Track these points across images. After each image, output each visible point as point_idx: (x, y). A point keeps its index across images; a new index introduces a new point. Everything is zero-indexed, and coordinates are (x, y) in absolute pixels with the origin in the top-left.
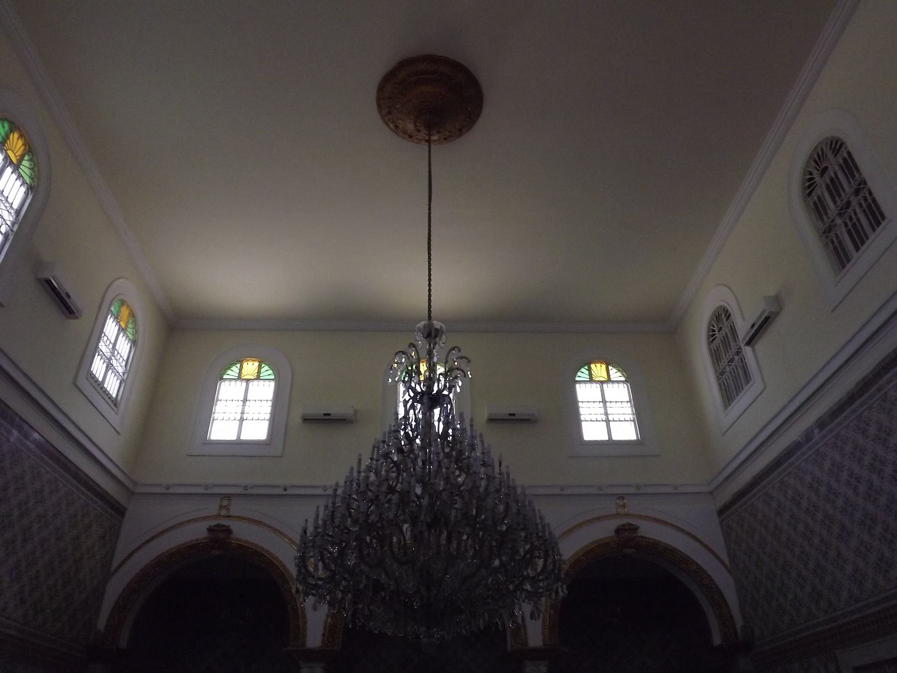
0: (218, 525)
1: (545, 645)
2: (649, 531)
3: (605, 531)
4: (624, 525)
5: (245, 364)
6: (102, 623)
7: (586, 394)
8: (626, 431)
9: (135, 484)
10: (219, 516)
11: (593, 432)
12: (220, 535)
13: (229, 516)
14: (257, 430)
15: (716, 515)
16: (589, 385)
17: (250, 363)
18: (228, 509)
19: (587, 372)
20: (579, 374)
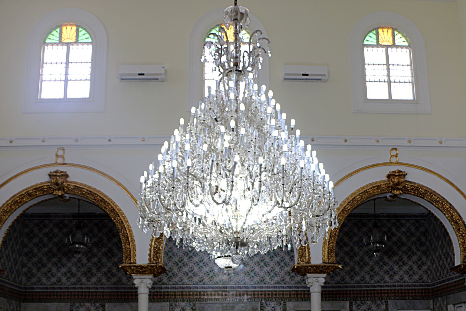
1: (324, 262)
2: (414, 177)
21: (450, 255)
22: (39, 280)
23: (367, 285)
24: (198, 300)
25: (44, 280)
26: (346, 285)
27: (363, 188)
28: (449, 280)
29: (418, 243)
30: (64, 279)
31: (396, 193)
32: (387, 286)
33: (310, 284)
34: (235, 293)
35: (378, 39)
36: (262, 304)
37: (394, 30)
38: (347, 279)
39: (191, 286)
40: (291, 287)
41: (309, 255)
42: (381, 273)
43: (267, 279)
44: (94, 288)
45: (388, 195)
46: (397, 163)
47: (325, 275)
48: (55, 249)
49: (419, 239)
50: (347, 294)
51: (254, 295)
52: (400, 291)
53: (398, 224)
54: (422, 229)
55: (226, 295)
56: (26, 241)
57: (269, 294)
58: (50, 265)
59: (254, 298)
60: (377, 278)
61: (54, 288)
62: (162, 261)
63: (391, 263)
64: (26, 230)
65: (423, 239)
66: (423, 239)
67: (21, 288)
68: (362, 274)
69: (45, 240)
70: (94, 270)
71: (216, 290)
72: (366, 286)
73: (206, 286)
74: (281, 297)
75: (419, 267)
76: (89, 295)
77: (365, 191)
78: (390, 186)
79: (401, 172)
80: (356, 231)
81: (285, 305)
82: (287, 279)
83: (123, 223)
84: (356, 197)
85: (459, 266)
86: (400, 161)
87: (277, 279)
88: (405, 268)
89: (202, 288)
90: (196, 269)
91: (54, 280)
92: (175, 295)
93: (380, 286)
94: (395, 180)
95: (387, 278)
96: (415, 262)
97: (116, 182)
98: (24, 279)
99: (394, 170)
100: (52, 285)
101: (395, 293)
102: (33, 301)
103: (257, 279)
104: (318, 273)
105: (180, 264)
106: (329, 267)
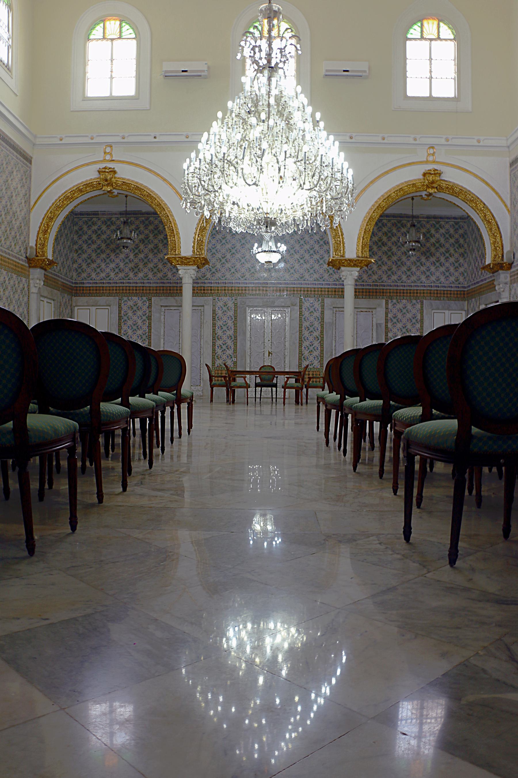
0: (105, 168)
2: (450, 176)
5: (107, 23)
6: (32, 243)
7: (415, 51)
8: (446, 88)
9: (35, 137)
10: (104, 160)
11: (416, 87)
12: (107, 177)
13: (113, 160)
14: (126, 86)
15: (508, 165)
16: (418, 42)
17: (113, 22)
18: (111, 154)
19: (419, 29)
20: (411, 31)
21: (483, 256)
22: (89, 276)
23: (403, 284)
24: (239, 294)
25: (94, 275)
27: (398, 186)
28: (482, 281)
29: (457, 245)
30: (112, 275)
31: (431, 191)
32: (423, 286)
33: (344, 277)
34: (275, 289)
35: (422, 31)
36: (301, 300)
37: (439, 21)
38: (385, 278)
39: (233, 281)
41: (344, 250)
42: (418, 273)
43: (307, 276)
44: (141, 283)
45: (424, 194)
46: (434, 162)
47: (358, 269)
48: (103, 246)
49: (457, 241)
50: (383, 292)
51: (293, 291)
52: (436, 292)
53: (438, 226)
54: (461, 231)
55: (266, 290)
56: (76, 238)
57: (308, 291)
58: (99, 261)
59: (294, 294)
60: (413, 278)
61: (103, 283)
62: (205, 254)
63: (428, 264)
64: (76, 228)
65: (461, 241)
66: (461, 241)
67: (72, 283)
68: (399, 273)
69: (94, 237)
70: (141, 266)
71: (257, 285)
72: (402, 286)
73: (247, 281)
74: (321, 293)
75: (456, 269)
76: (136, 290)
78: (425, 184)
79: (437, 170)
80: (394, 231)
81: (323, 301)
82: (326, 276)
83: (168, 217)
85: (489, 265)
86: (437, 160)
87: (316, 276)
88: (442, 269)
89: (244, 283)
90: (238, 266)
91: (103, 275)
92: (218, 290)
93: (416, 286)
94: (431, 178)
95: (423, 278)
96: (453, 264)
97: (162, 177)
98: (75, 274)
99: (429, 169)
100: (101, 280)
101: (430, 293)
102: (84, 295)
103: (296, 276)
104: (351, 266)
105: (223, 261)
106: (362, 260)
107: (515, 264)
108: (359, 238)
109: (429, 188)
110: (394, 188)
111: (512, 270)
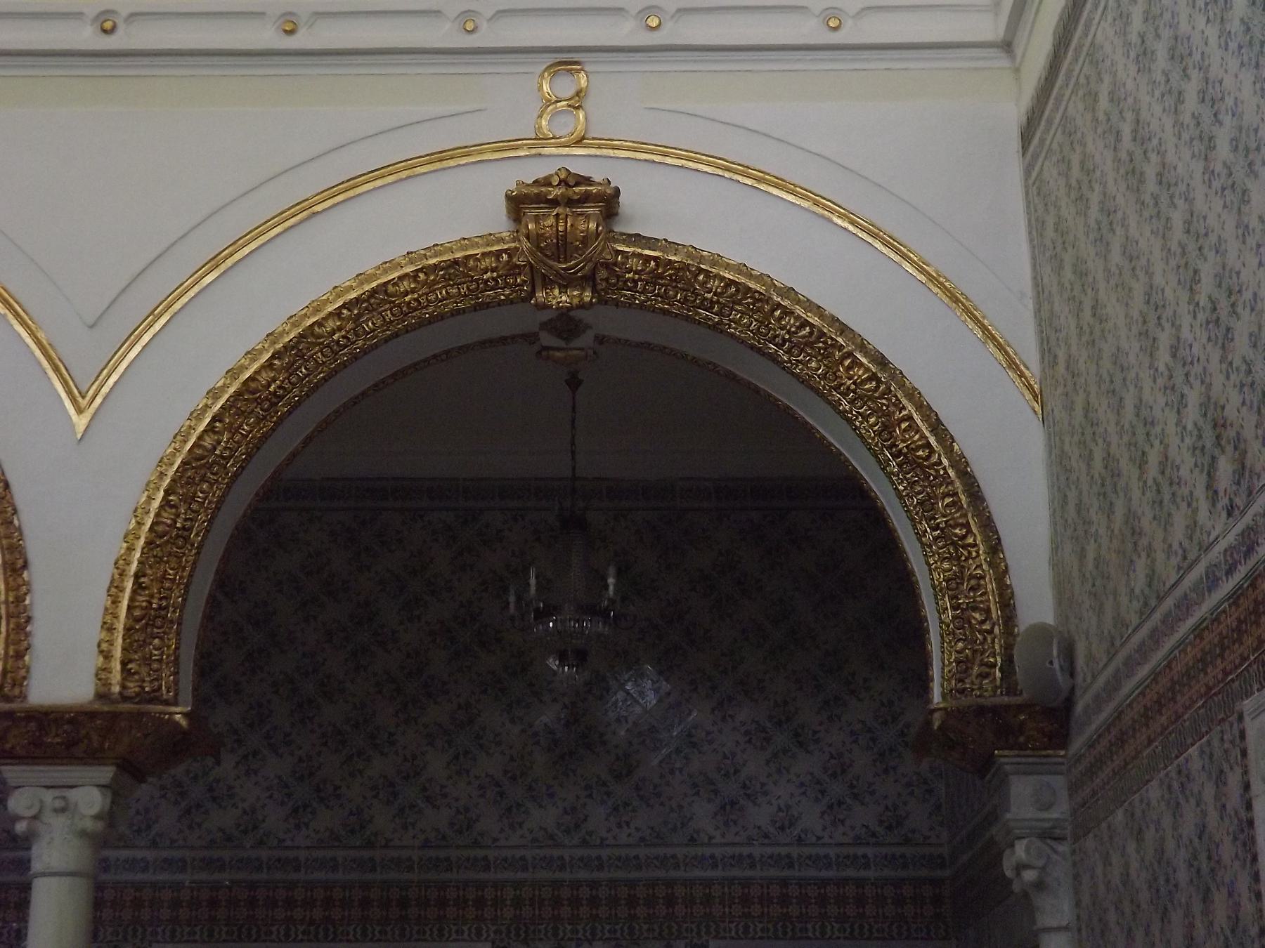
1: (101, 696)
3: (464, 214)
4: (547, 182)
15: (1015, 144)
23: (594, 853)
26: (480, 853)
40: (183, 865)
50: (480, 903)
52: (775, 891)
77: (374, 292)
78: (520, 261)
79: (588, 181)
84: (319, 324)
94: (548, 222)
95: (702, 813)
99: (541, 174)
107: (1079, 708)
108: (115, 588)
109: (547, 283)
110: (338, 291)
111: (1077, 744)
